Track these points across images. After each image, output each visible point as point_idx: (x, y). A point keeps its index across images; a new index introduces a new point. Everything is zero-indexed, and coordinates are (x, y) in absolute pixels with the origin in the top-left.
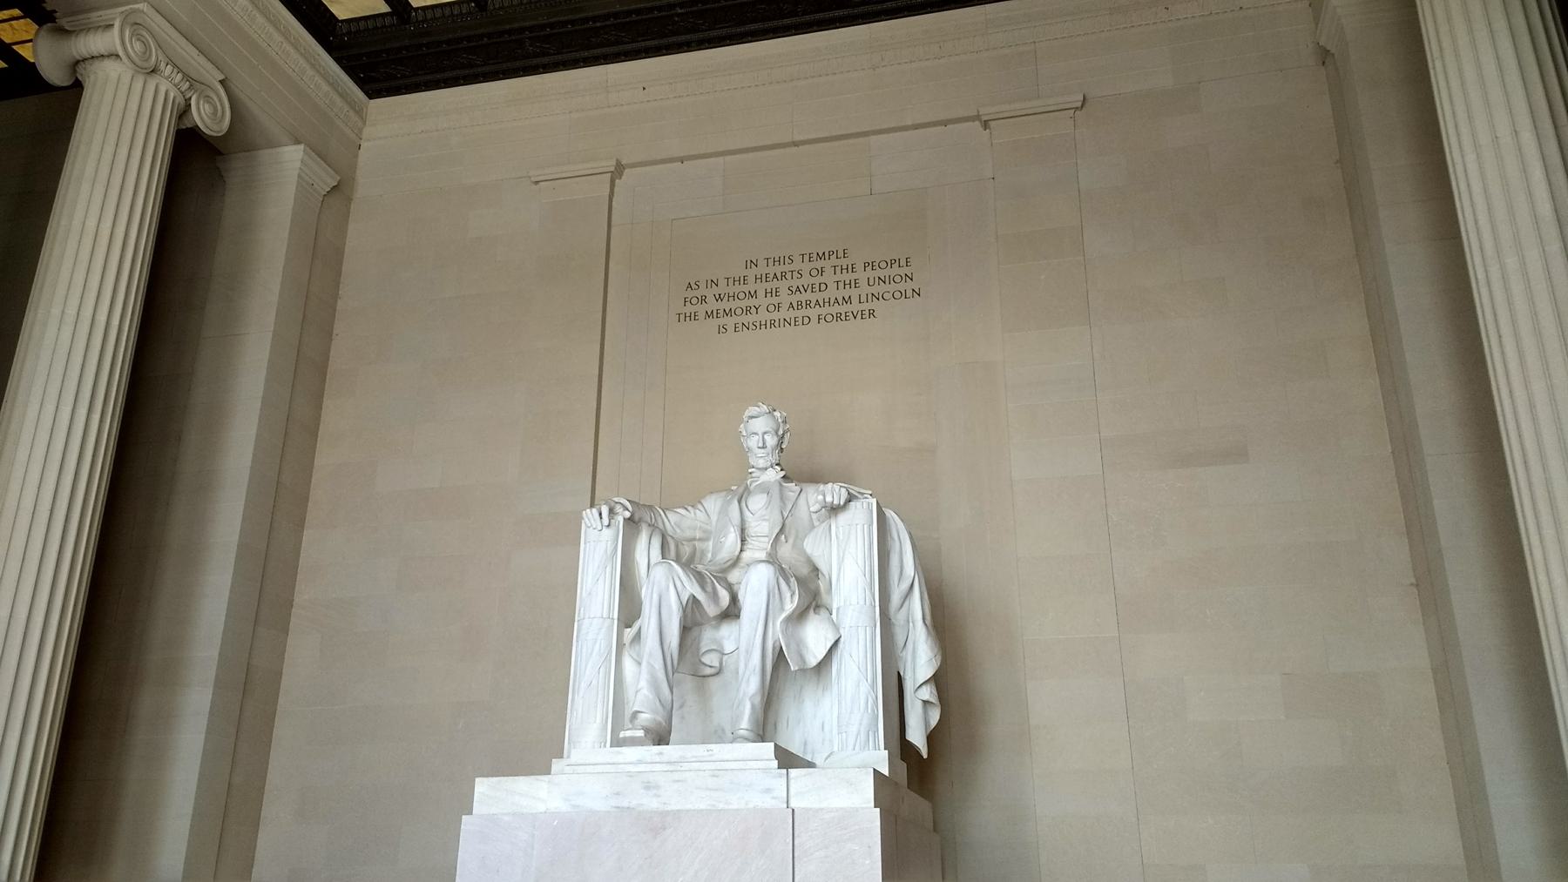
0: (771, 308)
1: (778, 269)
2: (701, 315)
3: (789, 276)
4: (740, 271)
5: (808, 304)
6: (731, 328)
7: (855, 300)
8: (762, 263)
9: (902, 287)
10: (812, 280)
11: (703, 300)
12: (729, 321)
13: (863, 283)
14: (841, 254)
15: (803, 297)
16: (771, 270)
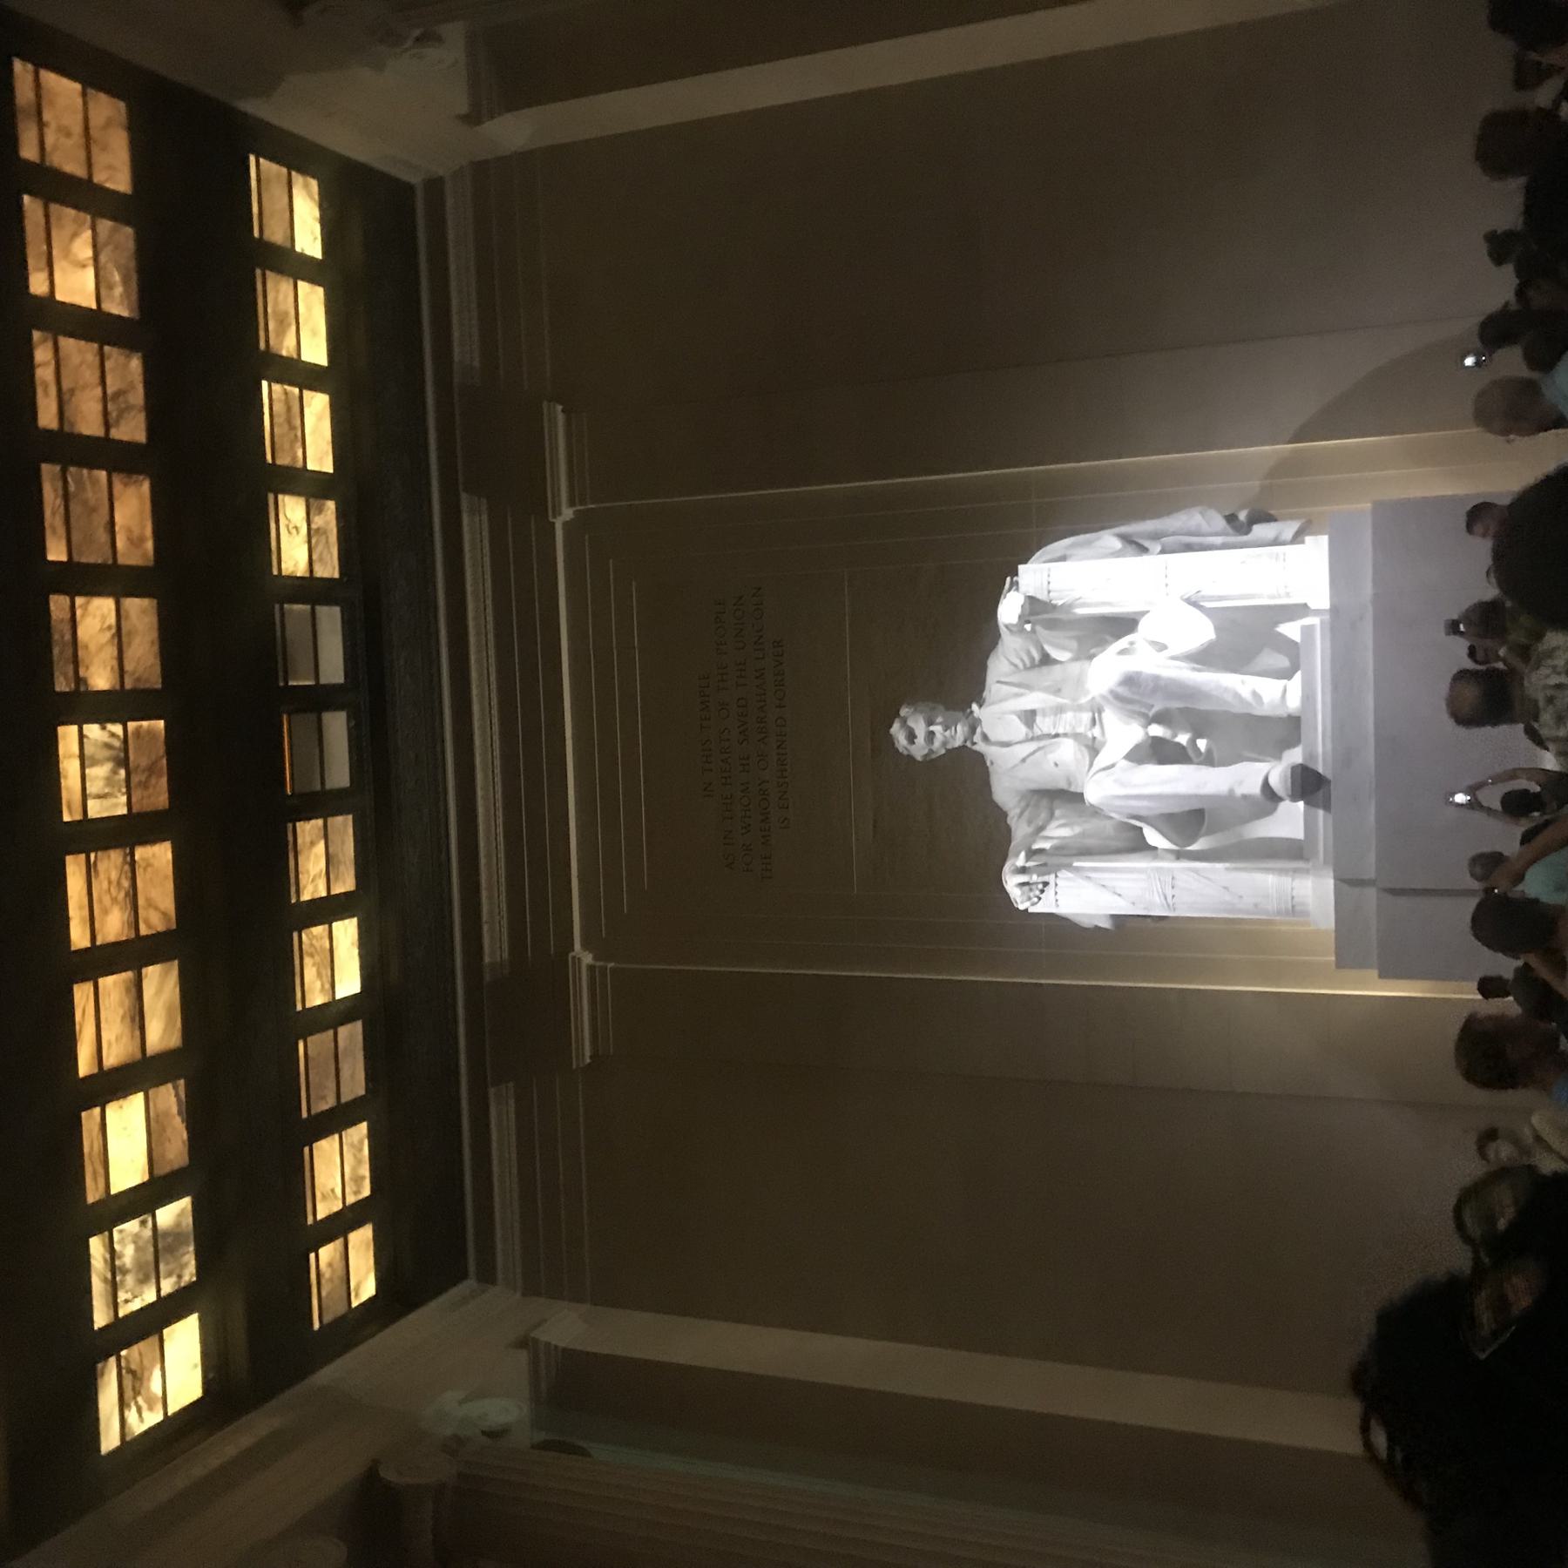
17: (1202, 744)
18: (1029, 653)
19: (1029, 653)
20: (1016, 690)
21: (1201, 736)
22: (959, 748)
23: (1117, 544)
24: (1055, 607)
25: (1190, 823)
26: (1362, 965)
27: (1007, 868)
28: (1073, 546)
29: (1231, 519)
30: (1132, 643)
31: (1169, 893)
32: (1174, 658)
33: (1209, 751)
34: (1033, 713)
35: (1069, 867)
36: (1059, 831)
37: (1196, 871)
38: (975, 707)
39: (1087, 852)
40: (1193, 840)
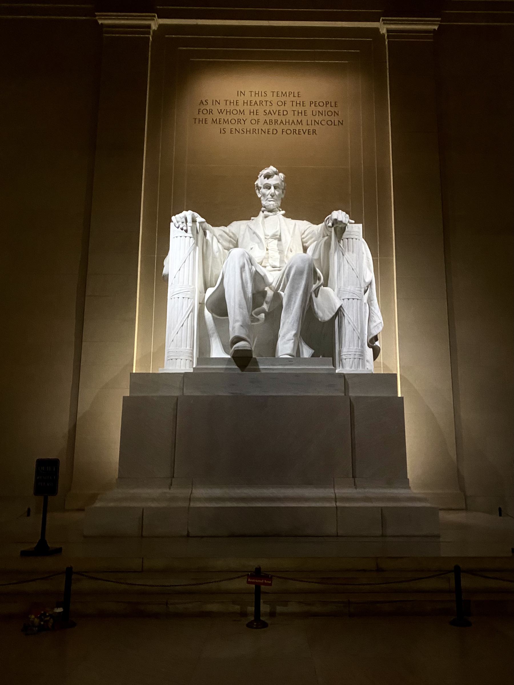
0: (253, 122)
1: (258, 99)
2: (209, 121)
3: (264, 103)
4: (233, 97)
5: (276, 122)
6: (228, 131)
7: (304, 122)
8: (247, 94)
9: (332, 118)
10: (278, 108)
11: (211, 112)
12: (228, 127)
13: (309, 113)
14: (296, 95)
15: (273, 117)
16: (254, 99)
17: (263, 315)
18: (311, 238)
19: (311, 238)
20: (291, 232)
21: (265, 316)
22: (261, 204)
23: (368, 280)
24: (339, 242)
25: (219, 306)
26: (133, 387)
27: (196, 214)
28: (368, 258)
29: (376, 338)
30: (319, 279)
31: (181, 296)
32: (311, 298)
33: (258, 320)
34: (280, 240)
35: (197, 244)
36: (216, 246)
37: (192, 311)
38: (283, 212)
39: (204, 257)
40: (211, 311)
